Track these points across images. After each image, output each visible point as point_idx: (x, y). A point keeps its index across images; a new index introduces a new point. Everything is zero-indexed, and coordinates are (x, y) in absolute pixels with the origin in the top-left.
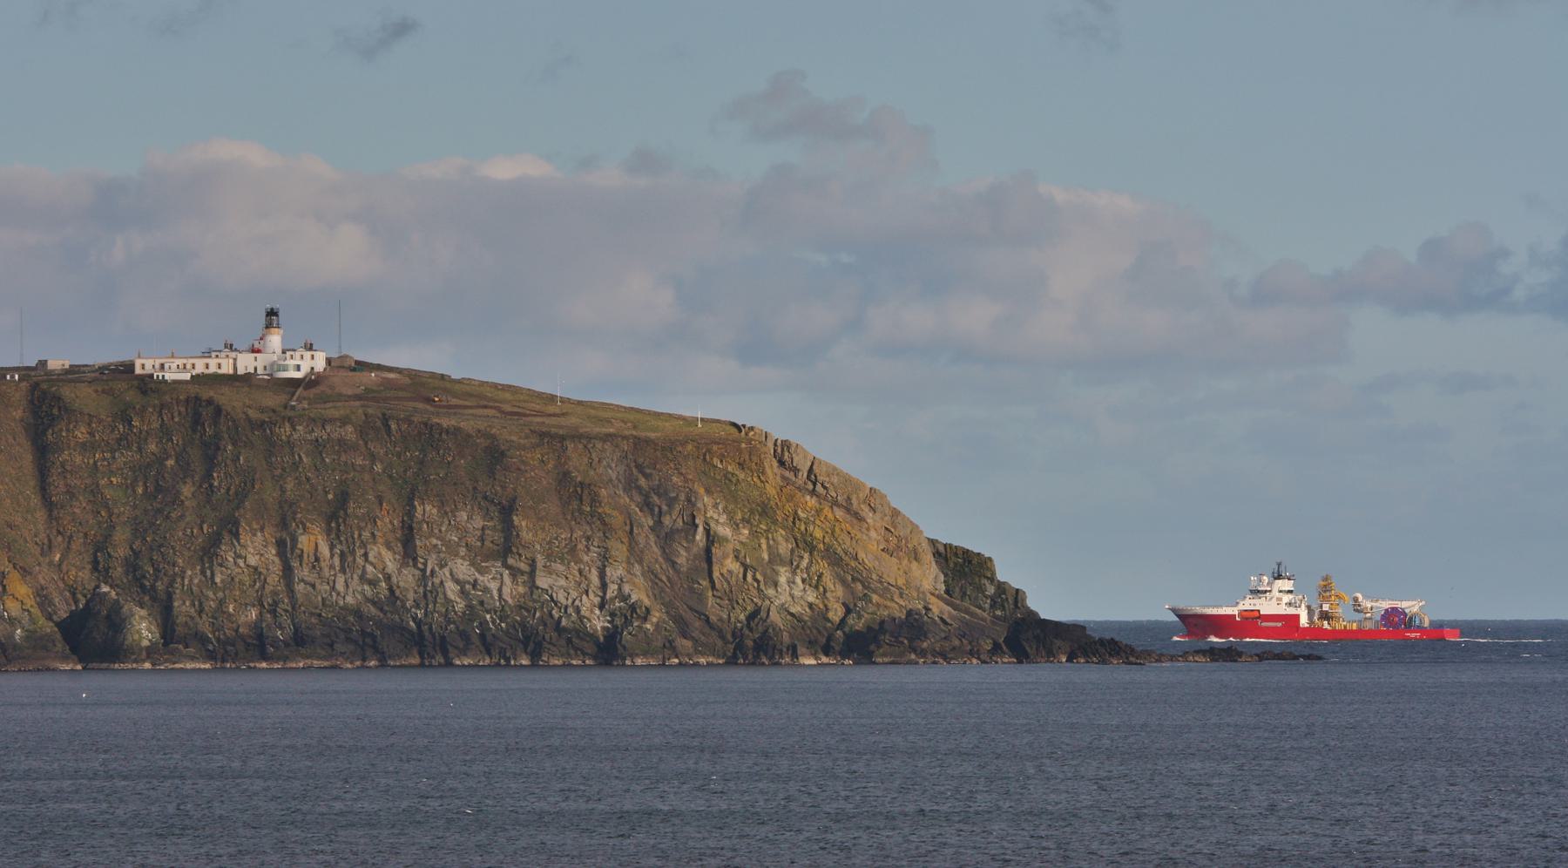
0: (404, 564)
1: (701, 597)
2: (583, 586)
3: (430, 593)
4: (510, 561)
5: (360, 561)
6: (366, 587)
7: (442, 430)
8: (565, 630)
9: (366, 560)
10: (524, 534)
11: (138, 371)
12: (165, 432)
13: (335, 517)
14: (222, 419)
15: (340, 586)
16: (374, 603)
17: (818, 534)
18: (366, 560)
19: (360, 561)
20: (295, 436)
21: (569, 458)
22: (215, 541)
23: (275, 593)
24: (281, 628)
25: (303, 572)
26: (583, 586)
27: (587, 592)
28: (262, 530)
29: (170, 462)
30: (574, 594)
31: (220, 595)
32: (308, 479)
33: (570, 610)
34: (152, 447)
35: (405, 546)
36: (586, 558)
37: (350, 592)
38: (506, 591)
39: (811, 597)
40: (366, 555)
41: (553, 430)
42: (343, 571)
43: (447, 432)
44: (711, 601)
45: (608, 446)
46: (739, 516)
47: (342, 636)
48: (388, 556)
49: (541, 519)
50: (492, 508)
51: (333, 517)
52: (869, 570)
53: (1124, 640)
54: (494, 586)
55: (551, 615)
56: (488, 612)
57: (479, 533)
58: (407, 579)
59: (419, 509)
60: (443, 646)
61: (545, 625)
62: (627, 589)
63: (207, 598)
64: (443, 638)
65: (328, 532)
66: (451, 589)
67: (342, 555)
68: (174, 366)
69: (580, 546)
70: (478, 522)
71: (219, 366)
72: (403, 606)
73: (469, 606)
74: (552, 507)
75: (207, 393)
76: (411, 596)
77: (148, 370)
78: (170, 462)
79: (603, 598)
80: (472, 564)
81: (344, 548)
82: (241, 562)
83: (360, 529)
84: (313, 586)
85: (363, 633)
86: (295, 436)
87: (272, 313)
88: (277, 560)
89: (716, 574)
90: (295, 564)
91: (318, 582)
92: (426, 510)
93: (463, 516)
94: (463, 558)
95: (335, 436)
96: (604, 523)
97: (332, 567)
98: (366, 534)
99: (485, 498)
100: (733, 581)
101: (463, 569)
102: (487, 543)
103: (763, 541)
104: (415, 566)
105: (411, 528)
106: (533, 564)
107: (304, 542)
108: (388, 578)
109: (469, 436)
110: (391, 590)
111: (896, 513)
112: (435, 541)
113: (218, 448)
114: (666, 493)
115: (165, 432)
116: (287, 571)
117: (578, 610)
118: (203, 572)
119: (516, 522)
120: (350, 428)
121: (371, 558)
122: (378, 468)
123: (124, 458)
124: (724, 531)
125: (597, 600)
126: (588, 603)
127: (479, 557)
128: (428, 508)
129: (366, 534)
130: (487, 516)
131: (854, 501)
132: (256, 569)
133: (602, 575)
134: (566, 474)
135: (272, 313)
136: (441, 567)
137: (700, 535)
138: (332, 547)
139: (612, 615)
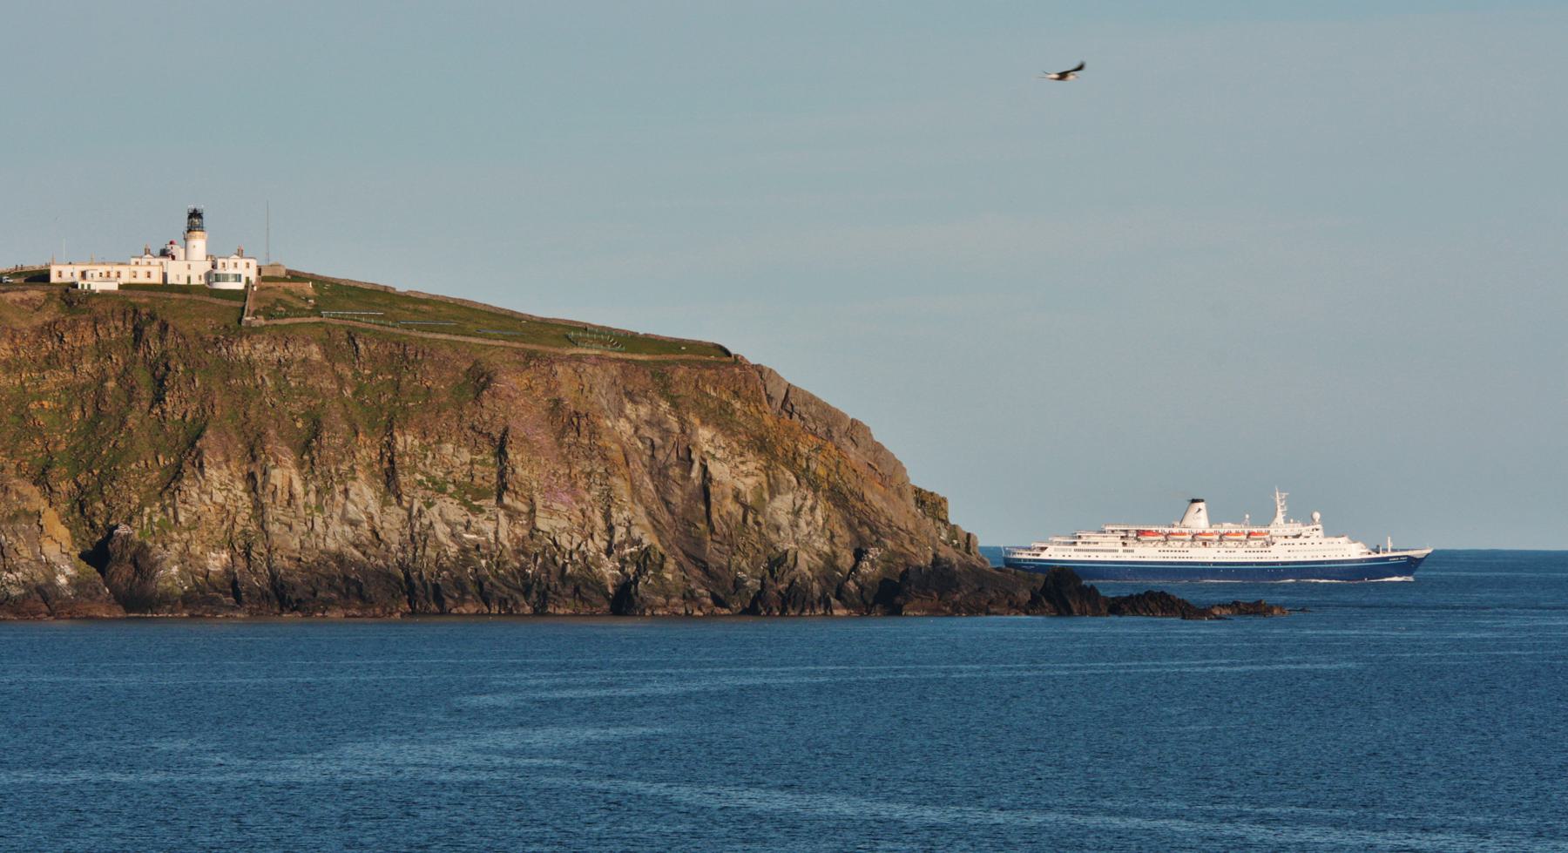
0: (385, 503)
1: (699, 543)
2: (588, 529)
3: (418, 538)
4: (507, 500)
5: (339, 498)
6: (347, 528)
8: (571, 577)
9: (347, 497)
10: (519, 470)
11: (54, 279)
12: (102, 350)
13: (307, 448)
14: (170, 336)
15: (319, 527)
16: (356, 547)
17: (822, 472)
18: (347, 497)
20: (255, 356)
21: (559, 384)
22: (177, 474)
23: (244, 532)
24: (256, 573)
25: (274, 512)
26: (588, 529)
28: (227, 461)
29: (111, 384)
30: (578, 539)
31: (186, 535)
33: (575, 556)
34: (87, 367)
35: (387, 485)
36: (588, 498)
37: (335, 537)
38: (502, 535)
40: (346, 491)
42: (319, 508)
44: (709, 546)
45: (598, 370)
47: (324, 583)
48: (368, 493)
49: (535, 453)
51: (307, 447)
52: (877, 513)
53: (1178, 589)
54: (489, 527)
55: (555, 563)
56: (483, 556)
57: (466, 468)
58: (392, 523)
59: (400, 440)
60: (438, 594)
61: (549, 572)
62: (636, 532)
64: (436, 587)
65: (300, 465)
67: (318, 492)
68: (97, 274)
69: (580, 484)
70: (466, 456)
72: (388, 549)
73: (464, 550)
74: (544, 438)
76: (395, 537)
77: (67, 278)
78: (111, 384)
79: (610, 543)
80: (465, 503)
81: (320, 483)
82: (206, 498)
83: (341, 462)
84: (290, 527)
85: (346, 578)
86: (255, 356)
88: (245, 496)
89: (715, 516)
90: (267, 500)
91: (294, 523)
92: (406, 441)
93: (448, 448)
94: (451, 495)
95: (299, 356)
96: (605, 458)
97: (306, 505)
98: (344, 467)
99: (473, 428)
100: (733, 524)
101: (454, 511)
102: (477, 480)
104: (400, 504)
105: (391, 462)
107: (278, 477)
108: (371, 518)
110: (375, 533)
111: (879, 448)
112: (419, 477)
115: (102, 350)
116: (259, 508)
117: (584, 556)
118: (164, 509)
119: (511, 456)
120: (314, 348)
121: (352, 495)
122: (348, 392)
123: (52, 380)
125: (603, 545)
127: (469, 495)
128: (409, 439)
129: (344, 467)
130: (475, 449)
131: (835, 434)
132: (223, 507)
133: (607, 516)
134: (558, 402)
135: (195, 214)
136: (429, 505)
137: (695, 472)
138: (305, 483)
139: (622, 561)
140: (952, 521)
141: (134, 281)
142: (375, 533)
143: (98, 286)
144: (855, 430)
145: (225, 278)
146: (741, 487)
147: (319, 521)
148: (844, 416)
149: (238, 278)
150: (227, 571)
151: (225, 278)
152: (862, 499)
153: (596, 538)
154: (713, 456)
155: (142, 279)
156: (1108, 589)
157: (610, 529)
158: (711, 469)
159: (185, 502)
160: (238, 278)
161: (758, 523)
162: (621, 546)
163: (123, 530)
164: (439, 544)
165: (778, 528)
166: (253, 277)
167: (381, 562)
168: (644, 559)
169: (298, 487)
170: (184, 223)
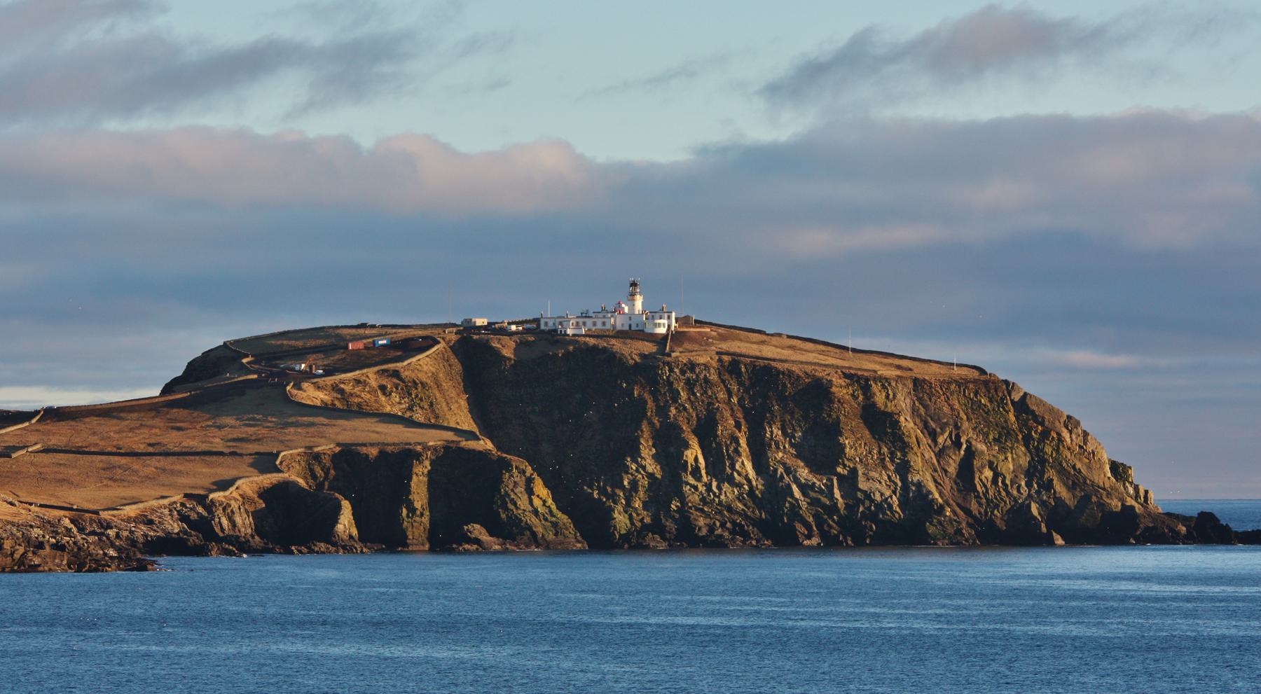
5: (728, 470)
7: (778, 372)
10: (847, 450)
11: (543, 327)
15: (714, 488)
19: (728, 470)
27: (894, 492)
32: (685, 409)
41: (860, 373)
43: (783, 373)
46: (991, 437)
47: (718, 524)
52: (1085, 479)
71: (604, 324)
75: (602, 344)
84: (696, 488)
85: (733, 522)
89: (977, 480)
96: (903, 442)
100: (989, 485)
103: (1009, 455)
106: (854, 472)
108: (749, 481)
109: (799, 377)
111: (1086, 434)
112: (780, 455)
114: (939, 419)
117: (890, 506)
121: (737, 467)
122: (735, 400)
124: (981, 447)
126: (895, 501)
133: (904, 479)
135: (634, 284)
147: (714, 484)
152: (1074, 467)
156: (1236, 527)
164: (797, 500)
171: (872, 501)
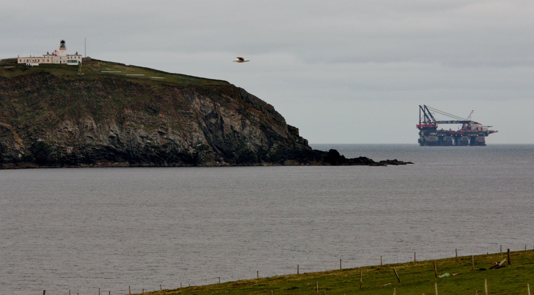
2: (185, 138)
11: (19, 62)
27: (186, 140)
33: (182, 147)
39: (258, 142)
40: (109, 127)
50: (152, 111)
52: (276, 133)
53: (370, 157)
55: (174, 148)
58: (123, 137)
59: (127, 112)
62: (200, 139)
63: (55, 143)
65: (95, 119)
66: (139, 140)
70: (148, 116)
71: (48, 61)
76: (125, 141)
77: (23, 62)
85: (110, 155)
87: (63, 42)
89: (225, 134)
99: (149, 108)
100: (230, 137)
106: (167, 130)
108: (117, 135)
111: (277, 113)
112: (133, 123)
113: (54, 89)
116: (82, 133)
117: (184, 146)
125: (190, 144)
132: (71, 132)
138: (96, 124)
140: (300, 135)
141: (44, 63)
142: (118, 140)
143: (33, 64)
144: (270, 109)
145: (73, 61)
146: (234, 126)
148: (266, 103)
149: (75, 61)
150: (73, 153)
151: (73, 61)
152: (271, 128)
153: (188, 142)
154: (225, 116)
155: (46, 62)
156: (348, 156)
157: (192, 139)
158: (223, 120)
159: (59, 131)
160: (75, 61)
161: (239, 137)
162: (196, 144)
163: (40, 140)
164: (139, 144)
165: (245, 138)
166: (81, 60)
167: (121, 150)
168: (202, 148)
169: (94, 125)
170: (59, 44)
171: (176, 144)
